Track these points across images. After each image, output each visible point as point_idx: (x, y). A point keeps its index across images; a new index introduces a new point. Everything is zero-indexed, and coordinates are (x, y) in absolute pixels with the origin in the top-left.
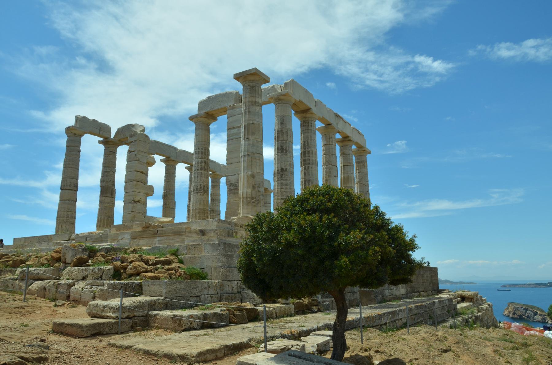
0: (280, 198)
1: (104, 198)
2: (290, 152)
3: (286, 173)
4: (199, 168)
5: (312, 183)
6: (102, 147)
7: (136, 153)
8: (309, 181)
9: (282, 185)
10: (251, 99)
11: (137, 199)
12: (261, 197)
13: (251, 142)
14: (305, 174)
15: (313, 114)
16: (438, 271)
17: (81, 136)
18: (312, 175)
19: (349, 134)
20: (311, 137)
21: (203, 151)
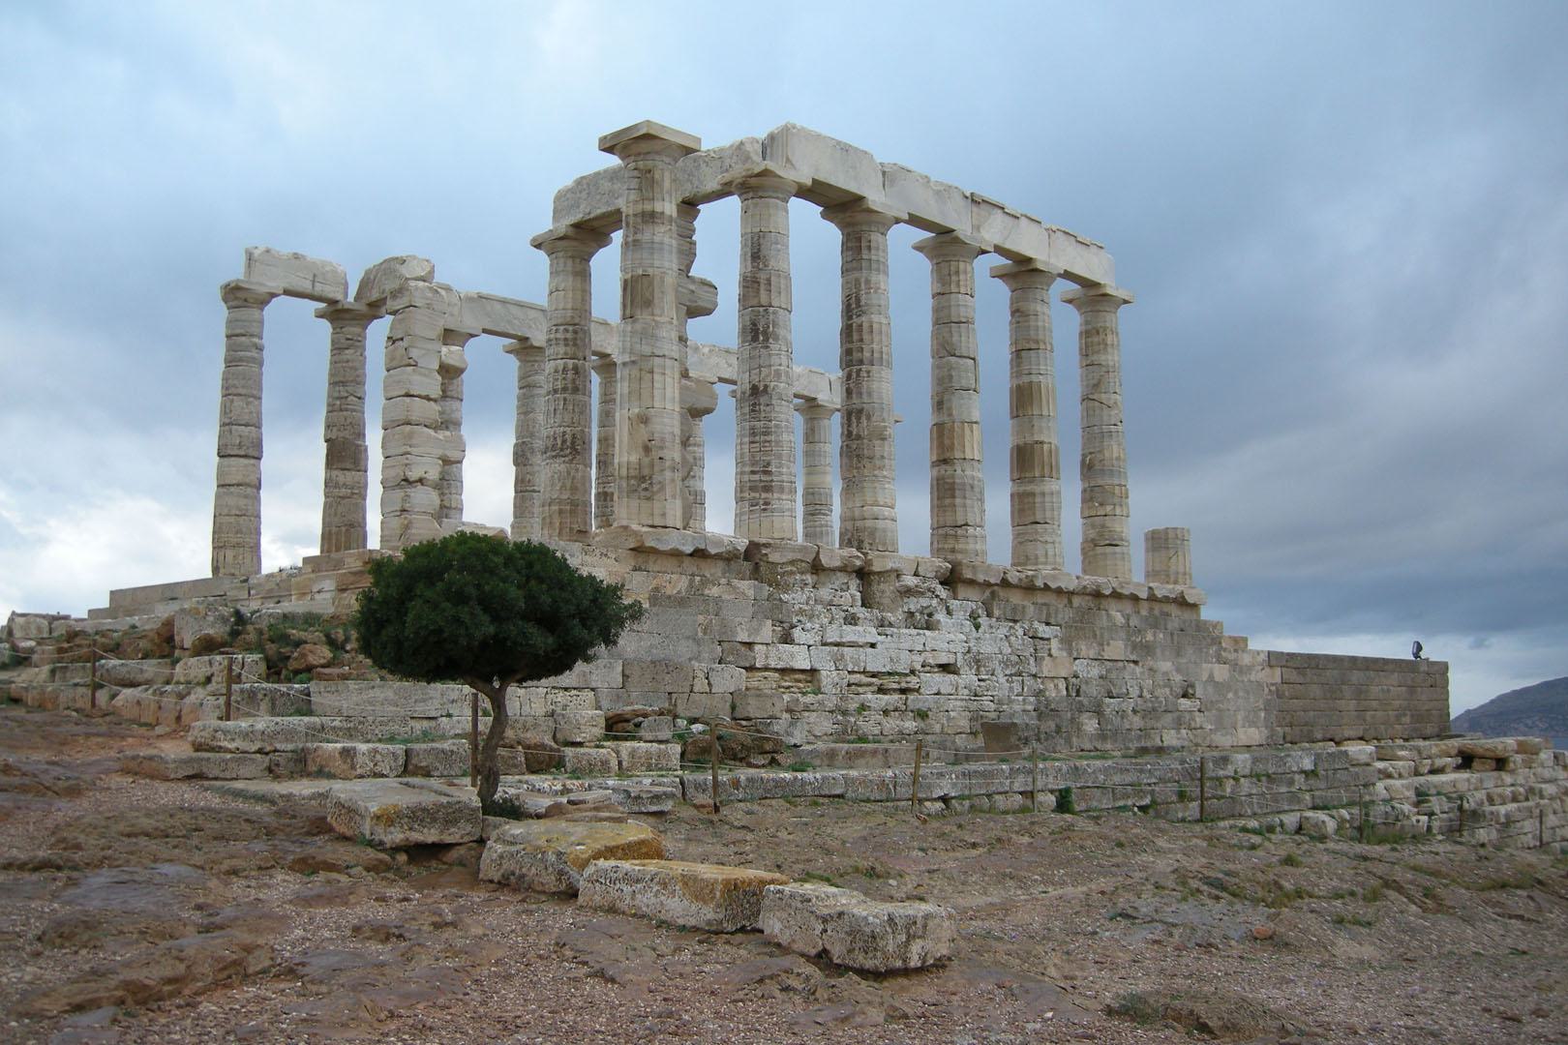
0: (748, 469)
1: (335, 473)
2: (777, 339)
3: (763, 400)
4: (559, 385)
5: (869, 418)
6: (326, 326)
7: (404, 344)
8: (860, 411)
9: (754, 434)
10: (639, 208)
11: (413, 475)
12: (668, 474)
13: (638, 326)
14: (849, 392)
15: (871, 211)
16: (1452, 676)
18: (870, 394)
19: (1029, 253)
20: (868, 282)
21: (569, 336)
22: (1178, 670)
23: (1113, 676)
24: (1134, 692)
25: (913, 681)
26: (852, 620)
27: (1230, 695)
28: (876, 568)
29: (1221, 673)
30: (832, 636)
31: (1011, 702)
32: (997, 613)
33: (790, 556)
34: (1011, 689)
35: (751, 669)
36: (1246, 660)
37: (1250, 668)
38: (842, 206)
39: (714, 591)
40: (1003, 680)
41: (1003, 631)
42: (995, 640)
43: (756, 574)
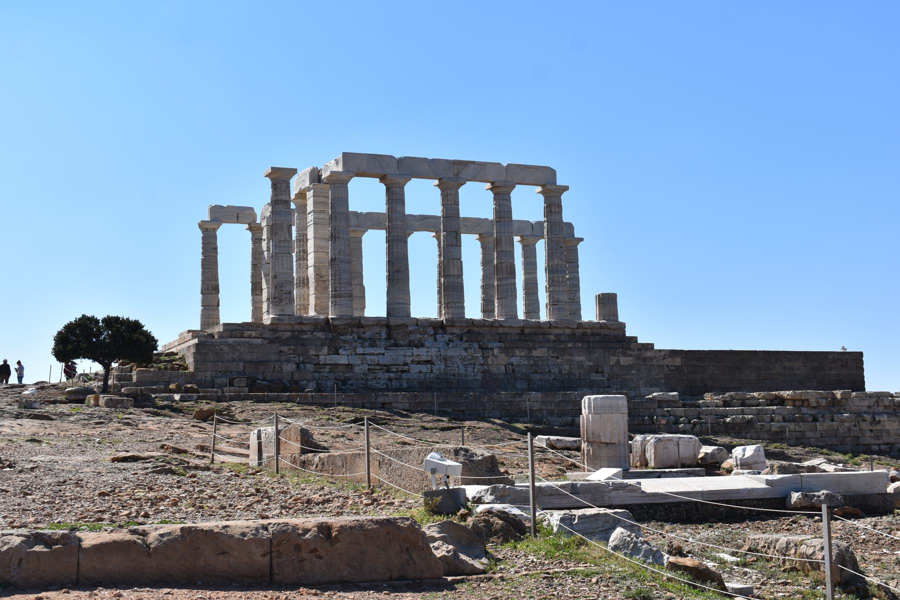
6: (249, 234)
16: (865, 359)
17: (215, 230)
22: (589, 361)
23: (540, 363)
24: (555, 370)
25: (406, 368)
26: (373, 345)
27: (633, 372)
28: (393, 322)
29: (624, 361)
30: (360, 350)
31: (466, 376)
32: (465, 338)
33: (345, 322)
34: (466, 370)
35: (318, 364)
36: (649, 354)
37: (652, 359)
38: (383, 179)
39: (305, 337)
40: (461, 366)
41: (466, 345)
42: (456, 352)
43: (330, 331)
